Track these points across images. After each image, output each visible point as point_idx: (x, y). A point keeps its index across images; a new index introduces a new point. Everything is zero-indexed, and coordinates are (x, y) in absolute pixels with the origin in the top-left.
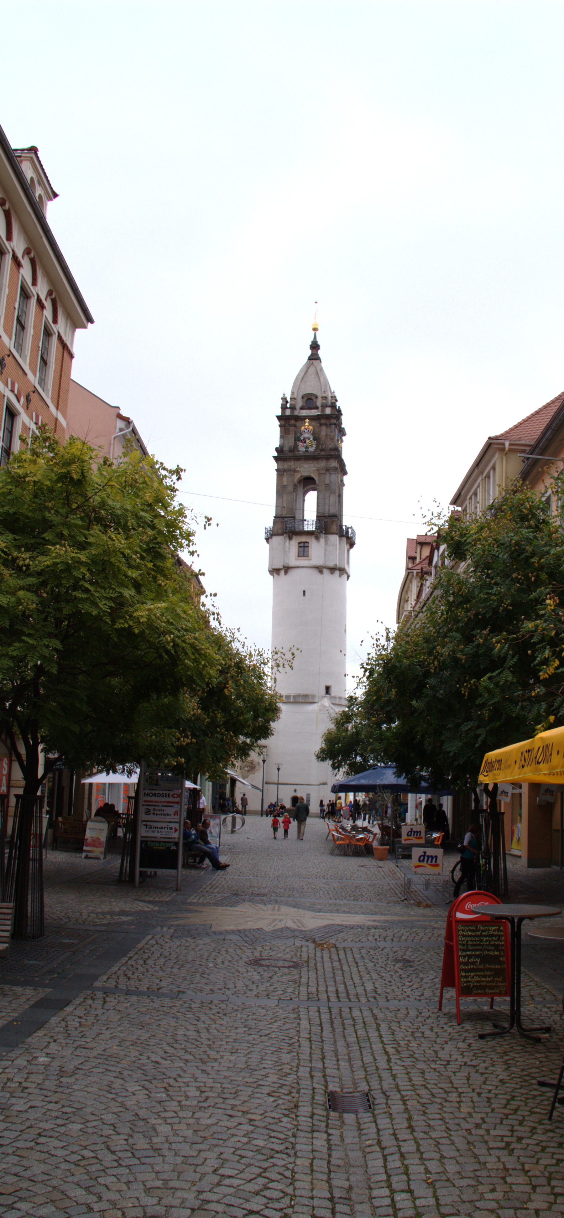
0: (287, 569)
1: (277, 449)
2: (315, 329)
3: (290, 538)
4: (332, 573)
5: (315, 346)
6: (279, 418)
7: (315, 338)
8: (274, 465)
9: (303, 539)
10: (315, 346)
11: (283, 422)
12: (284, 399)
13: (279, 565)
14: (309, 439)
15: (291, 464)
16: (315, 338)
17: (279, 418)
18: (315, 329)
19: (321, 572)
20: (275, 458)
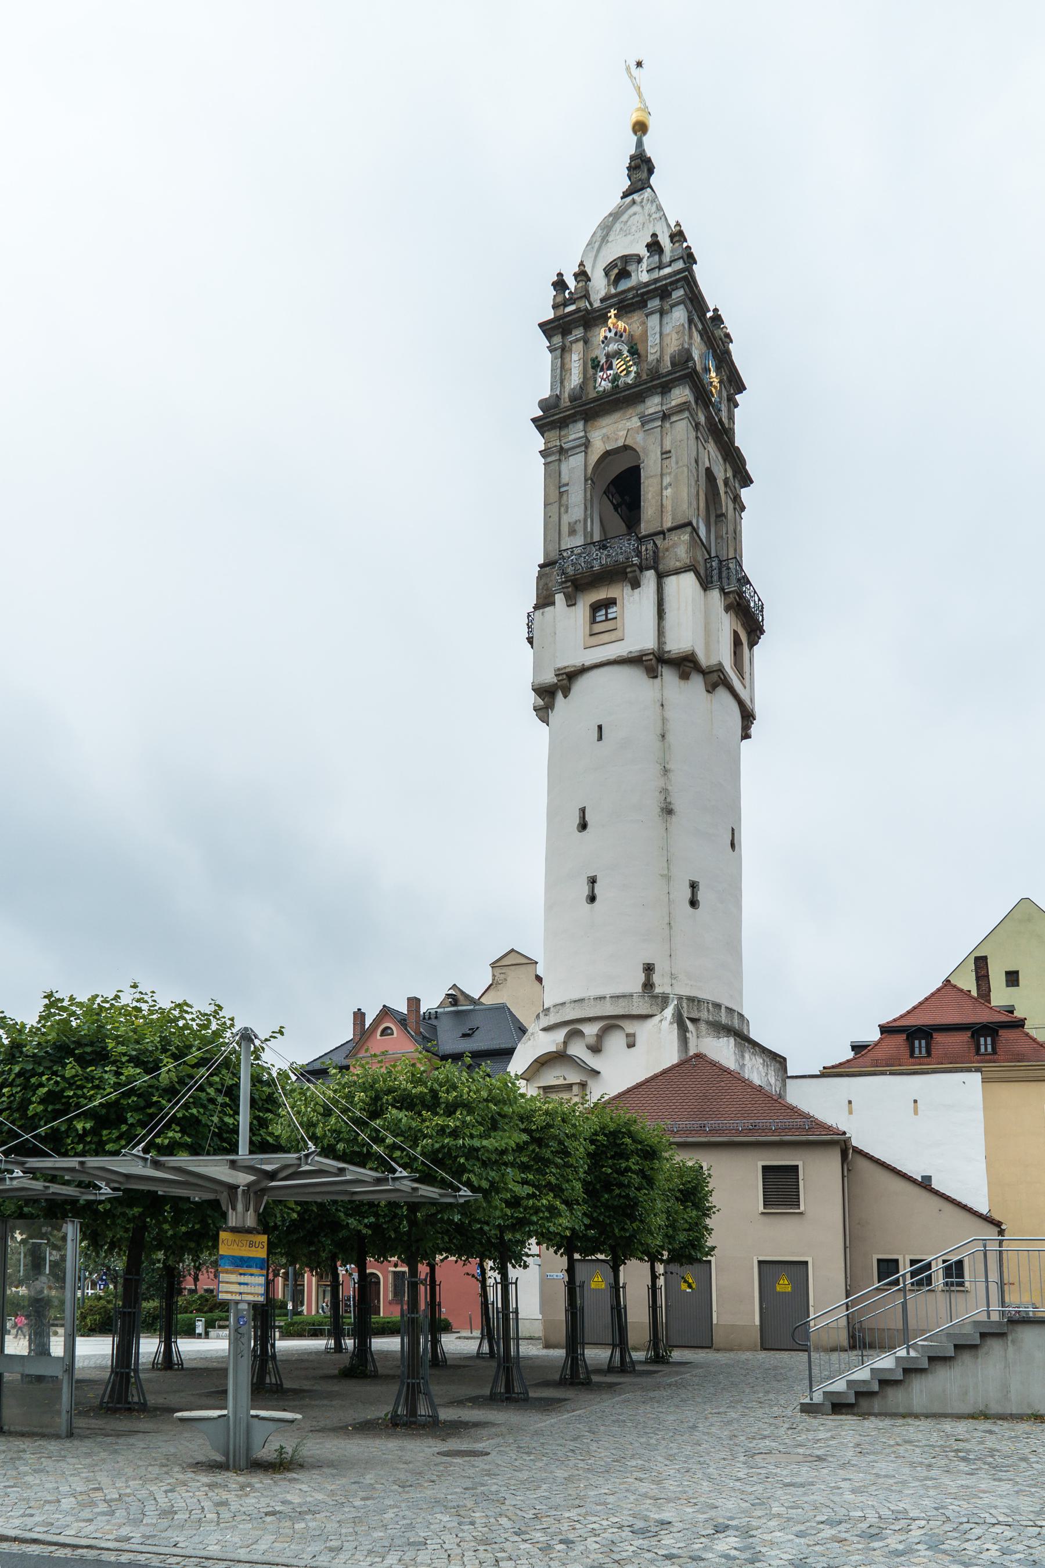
0: (569, 677)
1: (544, 405)
2: (640, 128)
3: (571, 602)
4: (684, 676)
5: (641, 168)
6: (548, 328)
7: (640, 144)
8: (539, 442)
9: (601, 594)
10: (641, 168)
11: (557, 340)
12: (560, 284)
15: (575, 432)
16: (640, 144)
17: (548, 328)
18: (640, 128)
19: (653, 673)
20: (542, 425)
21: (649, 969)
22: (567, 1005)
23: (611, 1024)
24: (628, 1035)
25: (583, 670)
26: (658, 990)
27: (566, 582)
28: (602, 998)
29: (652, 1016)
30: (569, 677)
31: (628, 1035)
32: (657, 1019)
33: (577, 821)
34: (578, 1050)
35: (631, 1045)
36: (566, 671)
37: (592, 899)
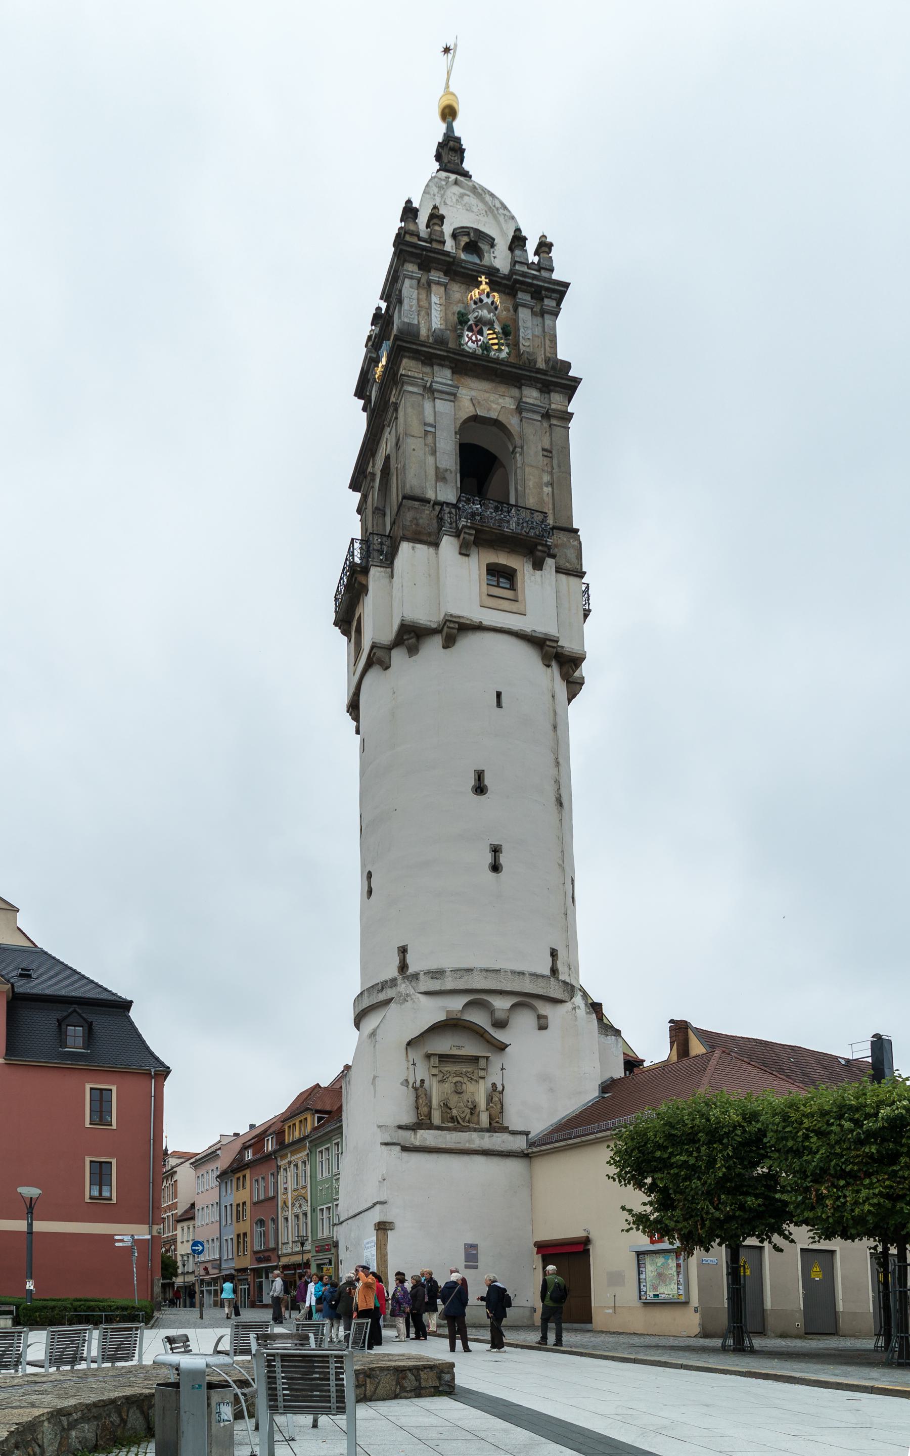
0: (454, 631)
2: (449, 113)
13: (424, 616)
14: (490, 325)
18: (449, 113)
21: (554, 954)
22: (475, 973)
23: (525, 1001)
24: (539, 1017)
25: (479, 628)
26: (561, 977)
27: (470, 528)
28: (521, 974)
29: (561, 1002)
30: (454, 631)
31: (539, 1017)
32: (568, 1006)
33: (472, 782)
34: (479, 1018)
35: (543, 1027)
36: (461, 621)
37: (496, 868)
